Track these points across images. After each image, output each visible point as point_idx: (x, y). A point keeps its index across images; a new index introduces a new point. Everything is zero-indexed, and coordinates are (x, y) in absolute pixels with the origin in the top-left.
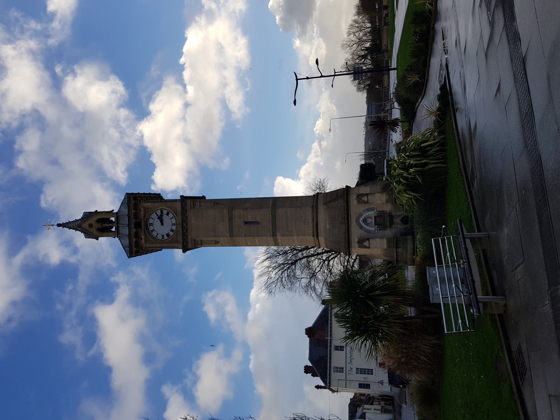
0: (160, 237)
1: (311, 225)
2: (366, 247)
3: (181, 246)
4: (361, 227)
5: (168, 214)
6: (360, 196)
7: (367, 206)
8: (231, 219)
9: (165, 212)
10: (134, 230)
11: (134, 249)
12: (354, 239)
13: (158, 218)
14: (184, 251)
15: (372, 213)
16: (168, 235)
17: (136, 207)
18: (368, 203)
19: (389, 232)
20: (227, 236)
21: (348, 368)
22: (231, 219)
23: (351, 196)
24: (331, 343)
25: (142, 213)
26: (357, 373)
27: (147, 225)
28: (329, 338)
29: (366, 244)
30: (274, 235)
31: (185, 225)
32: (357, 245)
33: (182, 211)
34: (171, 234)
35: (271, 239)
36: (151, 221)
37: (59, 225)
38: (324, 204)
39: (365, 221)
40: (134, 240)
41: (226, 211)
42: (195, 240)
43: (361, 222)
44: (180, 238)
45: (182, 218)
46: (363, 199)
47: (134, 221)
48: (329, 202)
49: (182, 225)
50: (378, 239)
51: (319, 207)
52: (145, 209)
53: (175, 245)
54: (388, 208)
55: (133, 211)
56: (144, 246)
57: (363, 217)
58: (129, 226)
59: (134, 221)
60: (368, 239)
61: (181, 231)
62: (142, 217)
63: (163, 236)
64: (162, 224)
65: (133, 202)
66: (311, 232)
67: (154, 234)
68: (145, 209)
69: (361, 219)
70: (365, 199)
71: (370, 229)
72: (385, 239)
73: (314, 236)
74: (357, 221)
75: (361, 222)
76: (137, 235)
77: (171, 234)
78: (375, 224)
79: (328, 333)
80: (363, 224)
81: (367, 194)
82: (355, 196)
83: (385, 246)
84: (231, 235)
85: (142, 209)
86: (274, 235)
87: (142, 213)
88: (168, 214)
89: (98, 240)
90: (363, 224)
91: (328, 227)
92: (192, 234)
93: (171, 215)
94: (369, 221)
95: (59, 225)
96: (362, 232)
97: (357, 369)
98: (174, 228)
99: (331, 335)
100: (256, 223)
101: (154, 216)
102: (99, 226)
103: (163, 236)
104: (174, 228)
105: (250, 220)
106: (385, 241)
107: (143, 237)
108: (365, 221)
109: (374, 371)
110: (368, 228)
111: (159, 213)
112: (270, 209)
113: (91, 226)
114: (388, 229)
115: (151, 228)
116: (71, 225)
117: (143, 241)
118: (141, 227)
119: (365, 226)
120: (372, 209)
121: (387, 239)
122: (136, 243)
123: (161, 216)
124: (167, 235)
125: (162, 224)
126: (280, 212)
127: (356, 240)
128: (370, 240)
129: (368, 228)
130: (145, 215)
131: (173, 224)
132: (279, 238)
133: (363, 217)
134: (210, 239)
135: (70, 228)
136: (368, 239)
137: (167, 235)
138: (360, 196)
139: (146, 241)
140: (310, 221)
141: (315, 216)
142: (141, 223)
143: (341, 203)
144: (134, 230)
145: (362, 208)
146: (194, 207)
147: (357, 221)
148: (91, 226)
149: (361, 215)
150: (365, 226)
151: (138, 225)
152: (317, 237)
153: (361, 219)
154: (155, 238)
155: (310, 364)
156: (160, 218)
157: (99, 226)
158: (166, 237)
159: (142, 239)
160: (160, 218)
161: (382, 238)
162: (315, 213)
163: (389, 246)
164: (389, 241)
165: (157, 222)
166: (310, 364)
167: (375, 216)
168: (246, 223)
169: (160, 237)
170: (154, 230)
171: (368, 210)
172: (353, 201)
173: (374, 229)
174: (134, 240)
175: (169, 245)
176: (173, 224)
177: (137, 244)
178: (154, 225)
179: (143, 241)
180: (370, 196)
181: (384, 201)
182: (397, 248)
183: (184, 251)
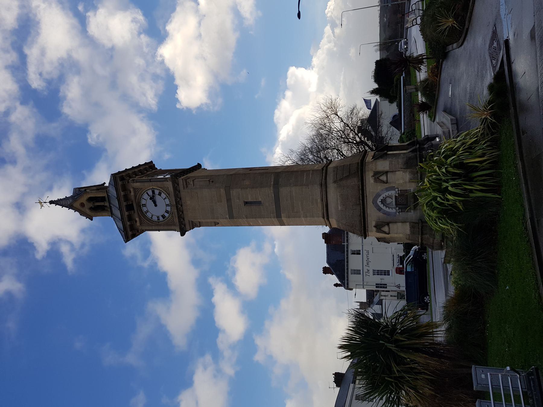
0: (155, 218)
1: (320, 205)
2: (385, 233)
3: (178, 229)
4: (380, 209)
5: (160, 194)
6: (377, 175)
7: (386, 186)
8: (229, 200)
9: (157, 192)
10: (127, 213)
11: (130, 233)
12: (372, 222)
13: (150, 199)
14: (183, 234)
15: (393, 193)
16: (163, 216)
17: (125, 188)
18: (387, 182)
19: (412, 215)
20: (226, 218)
21: (365, 270)
22: (229, 200)
23: (367, 173)
24: (347, 248)
25: (132, 194)
26: (374, 274)
27: (139, 206)
28: (346, 244)
29: (386, 229)
31: (180, 206)
32: (375, 229)
33: (175, 192)
34: (167, 215)
36: (143, 202)
38: (335, 182)
39: (383, 201)
40: (128, 223)
41: (222, 191)
42: (192, 222)
43: (380, 204)
44: (176, 220)
45: (176, 200)
46: (381, 178)
47: (125, 204)
48: (341, 180)
49: (177, 207)
50: (400, 224)
51: (328, 186)
53: (173, 227)
54: (412, 187)
55: (123, 194)
56: (140, 228)
58: (120, 209)
59: (125, 204)
60: (388, 224)
61: (176, 213)
62: (133, 198)
63: (158, 217)
64: (156, 205)
65: (120, 183)
66: (320, 213)
67: (149, 215)
69: (379, 200)
70: (384, 178)
71: (390, 210)
72: (408, 224)
73: (324, 218)
74: (374, 202)
75: (380, 204)
76: (130, 218)
77: (167, 215)
78: (396, 204)
79: (344, 239)
80: (382, 206)
81: (386, 173)
82: (371, 174)
83: (408, 231)
84: (231, 217)
85: (132, 190)
87: (132, 194)
88: (160, 194)
89: (92, 220)
90: (382, 206)
91: (340, 208)
92: (189, 216)
93: (163, 195)
94: (389, 201)
95: (51, 202)
96: (381, 214)
97: (374, 270)
98: (169, 209)
99: (347, 241)
100: (259, 203)
101: (145, 196)
102: (91, 205)
103: (158, 217)
104: (169, 209)
105: (250, 200)
106: (407, 227)
107: (137, 219)
108: (383, 201)
109: (390, 272)
110: (387, 209)
111: (150, 193)
112: (272, 188)
113: (82, 205)
114: (412, 211)
115: (145, 209)
117: (138, 224)
118: (133, 209)
119: (384, 208)
120: (393, 188)
121: (410, 223)
123: (153, 196)
124: (162, 216)
125: (156, 205)
126: (284, 191)
127: (374, 223)
128: (390, 225)
129: (387, 209)
130: (135, 197)
131: (167, 205)
132: (284, 219)
133: (381, 198)
134: (209, 221)
135: (63, 206)
136: (388, 224)
137: (162, 216)
138: (377, 175)
139: (141, 224)
140: (319, 200)
141: (324, 196)
142: (132, 204)
143: (354, 181)
144: (127, 213)
145: (380, 187)
146: (187, 187)
147: (374, 202)
148: (82, 205)
149: (378, 195)
150: (384, 208)
151: (130, 208)
152: (328, 219)
153: (379, 200)
154: (150, 220)
155: (327, 266)
156: (153, 199)
157: (91, 205)
159: (136, 221)
160: (153, 199)
161: (404, 222)
162: (324, 193)
163: (413, 233)
164: (412, 227)
165: (150, 203)
166: (327, 266)
167: (396, 197)
168: (246, 203)
170: (147, 211)
171: (388, 189)
172: (369, 180)
173: (394, 210)
174: (128, 223)
175: (165, 228)
176: (167, 205)
177: (132, 227)
179: (138, 224)
180: (389, 175)
181: (407, 180)
182: (422, 234)
183: (183, 234)
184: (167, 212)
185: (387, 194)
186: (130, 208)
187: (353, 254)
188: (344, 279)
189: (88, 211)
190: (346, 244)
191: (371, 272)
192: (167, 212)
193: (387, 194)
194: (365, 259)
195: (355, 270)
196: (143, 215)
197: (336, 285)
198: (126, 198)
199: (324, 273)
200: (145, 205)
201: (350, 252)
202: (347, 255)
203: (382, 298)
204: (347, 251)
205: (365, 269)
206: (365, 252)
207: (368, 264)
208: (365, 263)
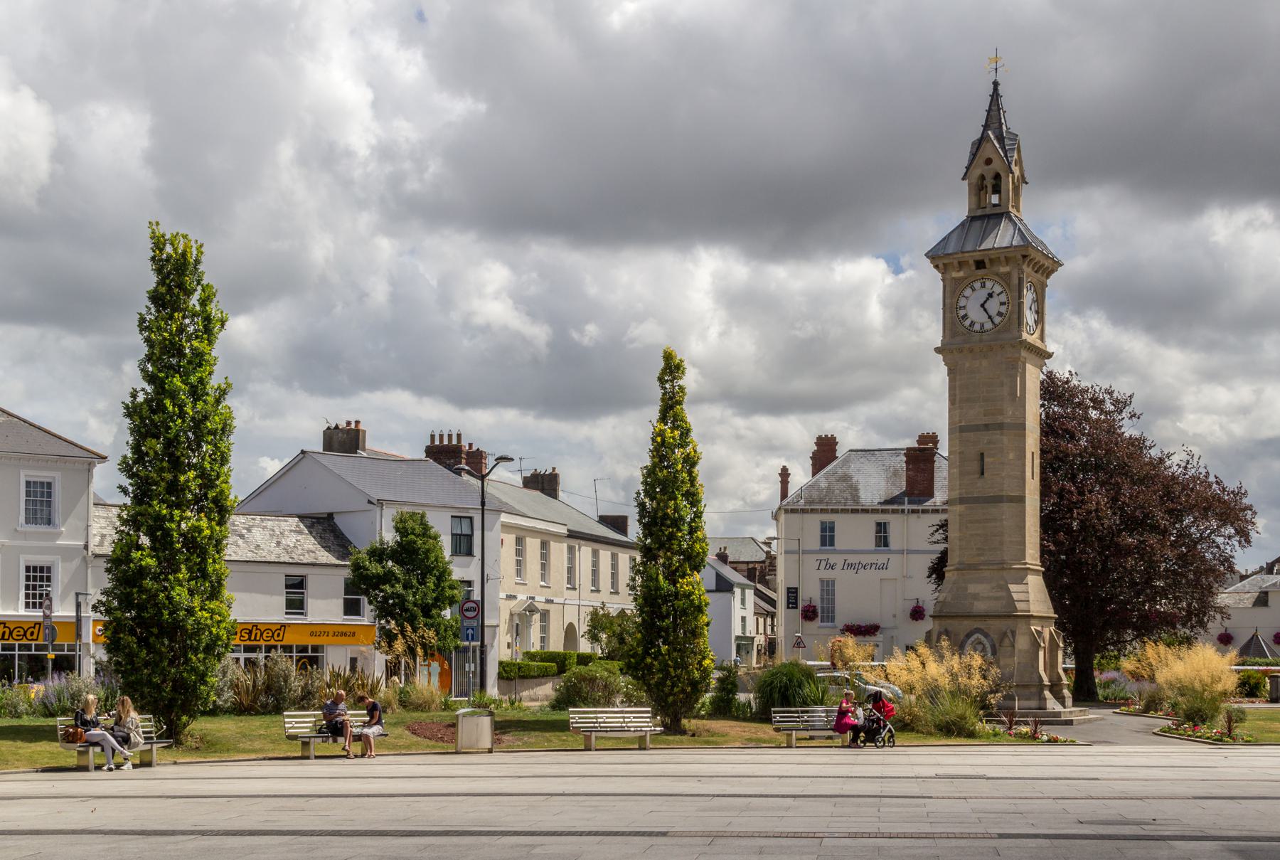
0: (962, 302)
4: (968, 636)
24: (894, 511)
30: (962, 501)
34: (967, 323)
35: (956, 494)
37: (996, 84)
62: (995, 269)
67: (968, 292)
75: (976, 636)
76: (961, 265)
77: (967, 323)
84: (962, 429)
86: (962, 501)
90: (972, 639)
95: (996, 84)
96: (962, 637)
98: (977, 327)
99: (913, 511)
103: (964, 307)
105: (986, 460)
113: (989, 162)
135: (989, 111)
149: (986, 635)
151: (980, 264)
158: (962, 313)
169: (962, 302)
184: (972, 324)
186: (980, 264)
187: (879, 524)
189: (976, 173)
190: (907, 507)
191: (828, 574)
192: (972, 324)
194: (865, 559)
195: (832, 529)
197: (785, 474)
199: (819, 438)
203: (737, 591)
206: (881, 559)
207: (851, 566)
208: (852, 559)
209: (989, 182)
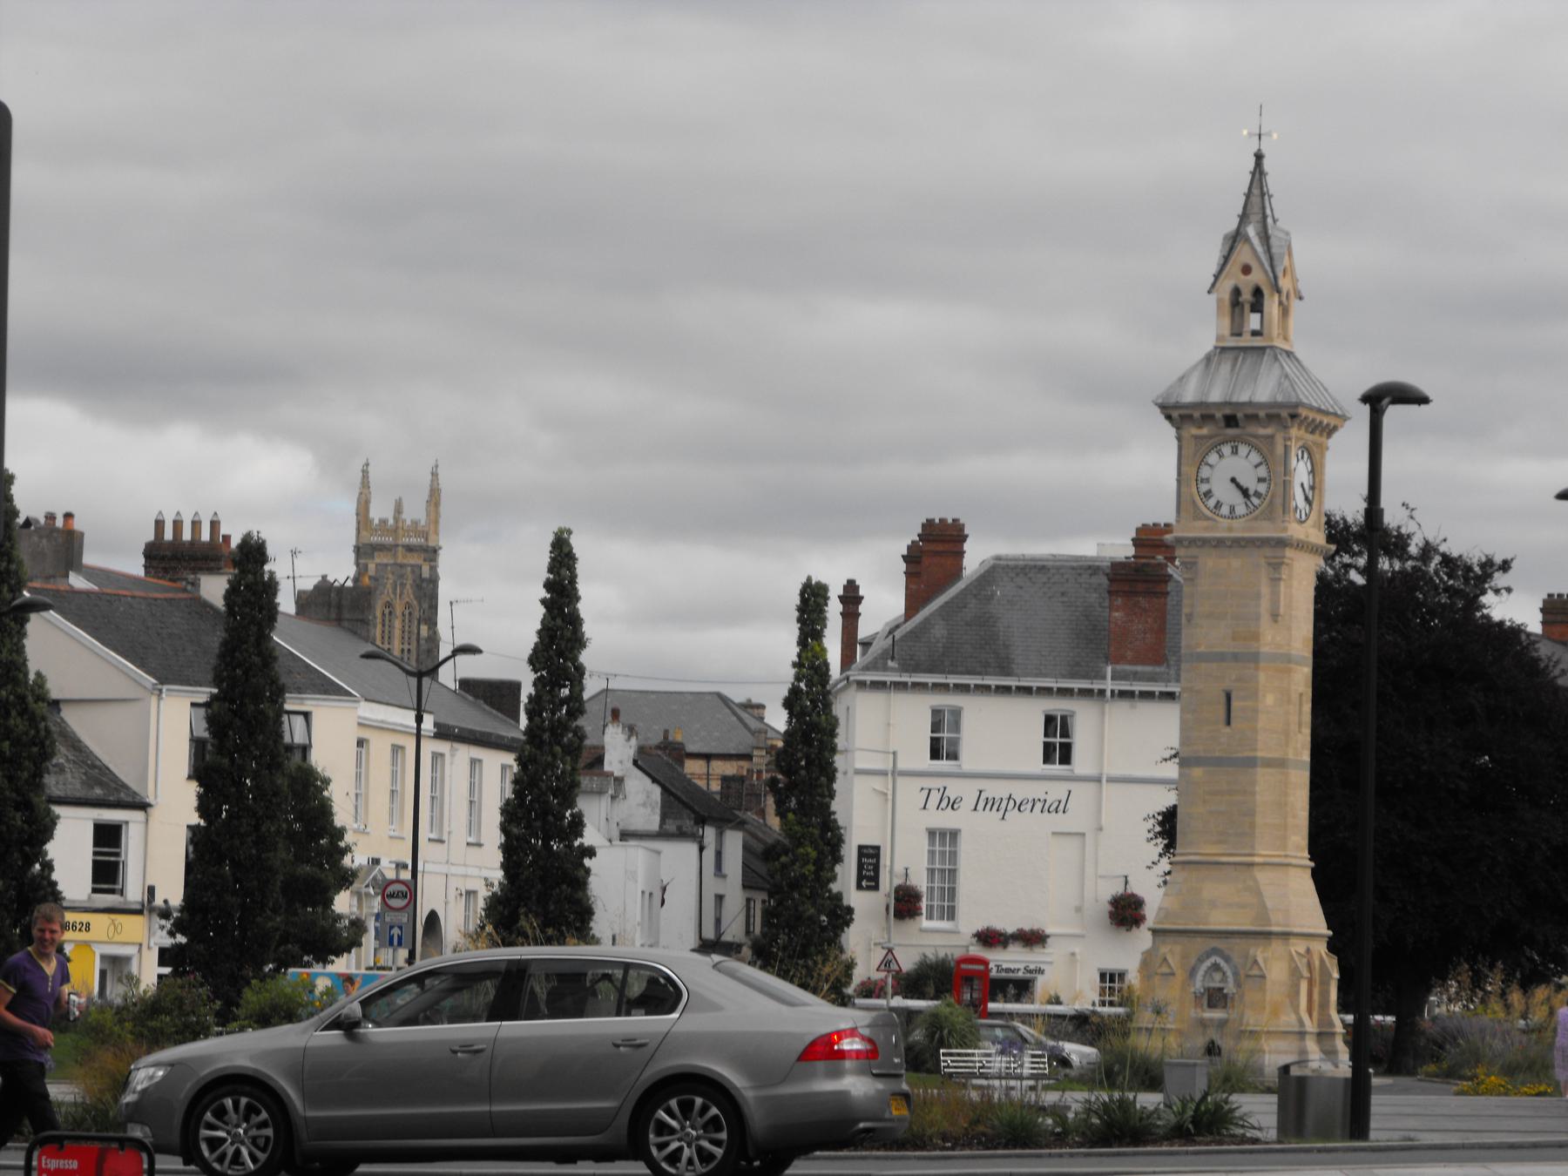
11: (1175, 414)
27: (1234, 443)
33: (1258, 539)
39: (1216, 967)
52: (1272, 437)
55: (1262, 414)
57: (1223, 964)
63: (1207, 480)
64: (1233, 480)
68: (1272, 437)
75: (1213, 959)
76: (1207, 418)
77: (1212, 503)
80: (1208, 963)
90: (1208, 963)
94: (1218, 976)
103: (1207, 480)
105: (1235, 704)
108: (1216, 967)
110: (1201, 973)
115: (1226, 449)
116: (1255, 200)
122: (1190, 417)
125: (1233, 480)
130: (1256, 437)
133: (1223, 964)
139: (1196, 437)
149: (1227, 959)
178: (1235, 458)
179: (1195, 431)
185: (1229, 973)
186: (1231, 421)
188: (906, 668)
191: (946, 820)
193: (1229, 973)
196: (1216, 447)
198: (1253, 418)
200: (1235, 452)
201: (1057, 706)
202: (1046, 692)
204: (1065, 692)
205: (965, 791)
207: (991, 803)
209: (1247, 296)
